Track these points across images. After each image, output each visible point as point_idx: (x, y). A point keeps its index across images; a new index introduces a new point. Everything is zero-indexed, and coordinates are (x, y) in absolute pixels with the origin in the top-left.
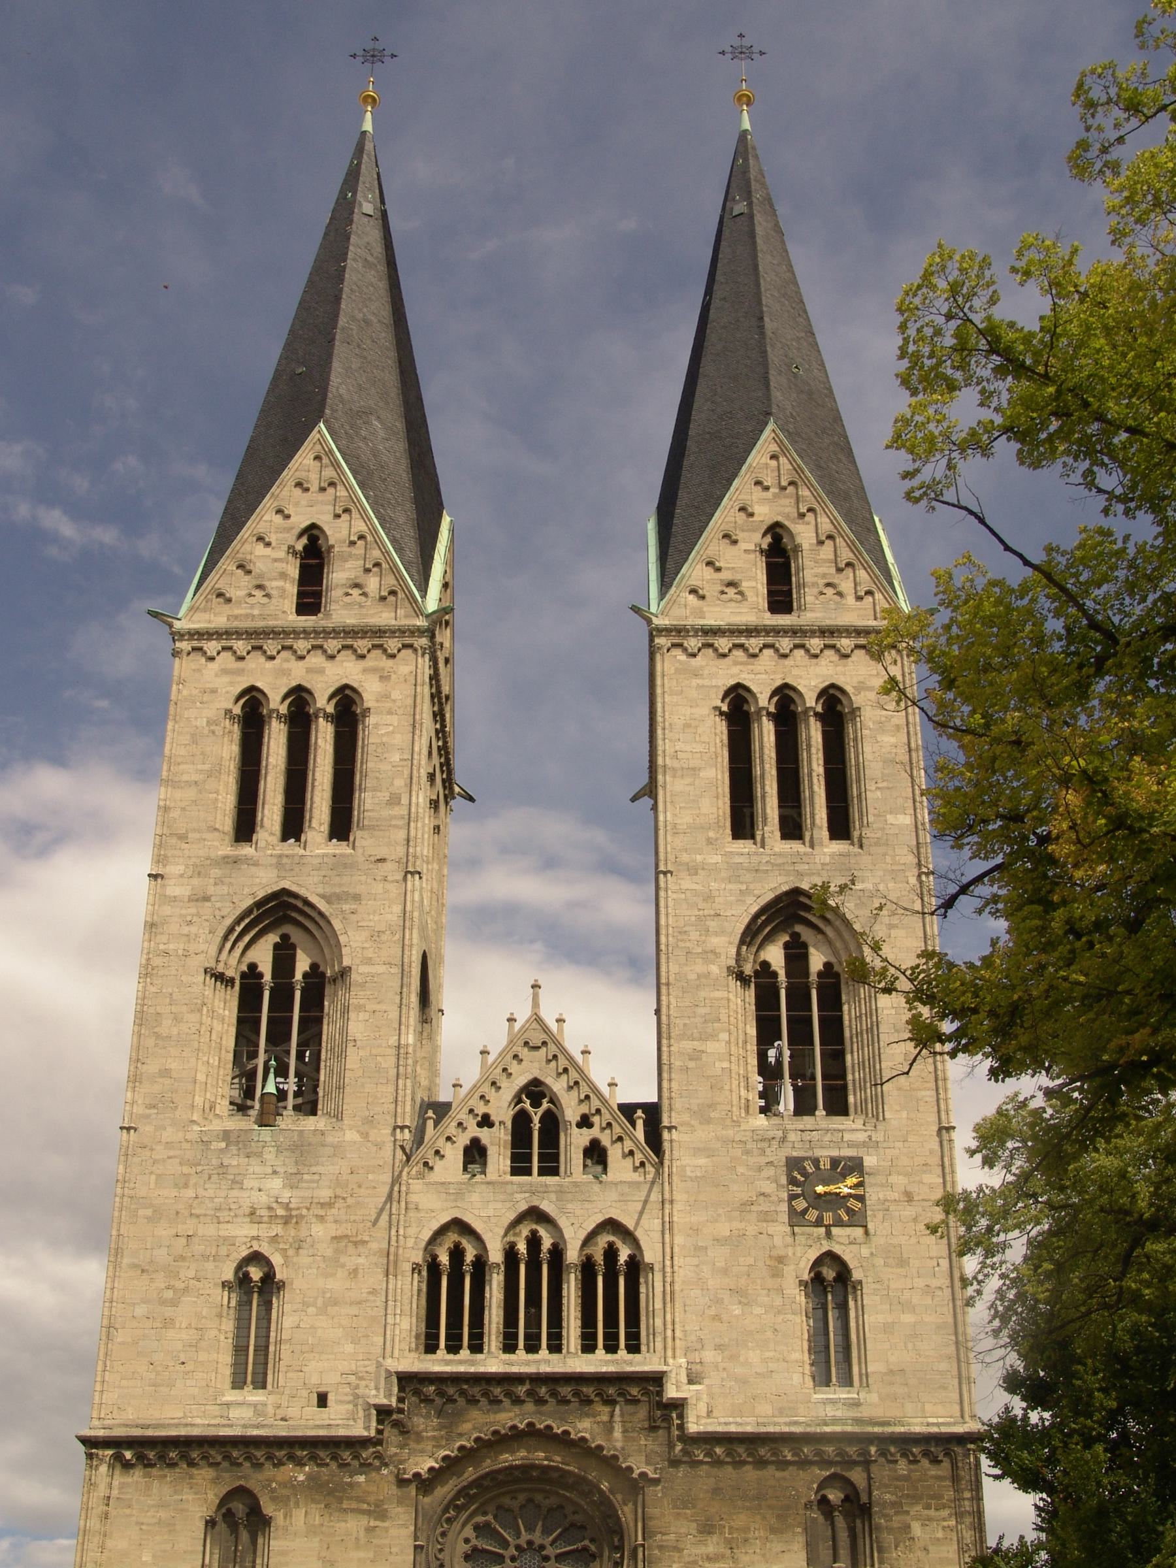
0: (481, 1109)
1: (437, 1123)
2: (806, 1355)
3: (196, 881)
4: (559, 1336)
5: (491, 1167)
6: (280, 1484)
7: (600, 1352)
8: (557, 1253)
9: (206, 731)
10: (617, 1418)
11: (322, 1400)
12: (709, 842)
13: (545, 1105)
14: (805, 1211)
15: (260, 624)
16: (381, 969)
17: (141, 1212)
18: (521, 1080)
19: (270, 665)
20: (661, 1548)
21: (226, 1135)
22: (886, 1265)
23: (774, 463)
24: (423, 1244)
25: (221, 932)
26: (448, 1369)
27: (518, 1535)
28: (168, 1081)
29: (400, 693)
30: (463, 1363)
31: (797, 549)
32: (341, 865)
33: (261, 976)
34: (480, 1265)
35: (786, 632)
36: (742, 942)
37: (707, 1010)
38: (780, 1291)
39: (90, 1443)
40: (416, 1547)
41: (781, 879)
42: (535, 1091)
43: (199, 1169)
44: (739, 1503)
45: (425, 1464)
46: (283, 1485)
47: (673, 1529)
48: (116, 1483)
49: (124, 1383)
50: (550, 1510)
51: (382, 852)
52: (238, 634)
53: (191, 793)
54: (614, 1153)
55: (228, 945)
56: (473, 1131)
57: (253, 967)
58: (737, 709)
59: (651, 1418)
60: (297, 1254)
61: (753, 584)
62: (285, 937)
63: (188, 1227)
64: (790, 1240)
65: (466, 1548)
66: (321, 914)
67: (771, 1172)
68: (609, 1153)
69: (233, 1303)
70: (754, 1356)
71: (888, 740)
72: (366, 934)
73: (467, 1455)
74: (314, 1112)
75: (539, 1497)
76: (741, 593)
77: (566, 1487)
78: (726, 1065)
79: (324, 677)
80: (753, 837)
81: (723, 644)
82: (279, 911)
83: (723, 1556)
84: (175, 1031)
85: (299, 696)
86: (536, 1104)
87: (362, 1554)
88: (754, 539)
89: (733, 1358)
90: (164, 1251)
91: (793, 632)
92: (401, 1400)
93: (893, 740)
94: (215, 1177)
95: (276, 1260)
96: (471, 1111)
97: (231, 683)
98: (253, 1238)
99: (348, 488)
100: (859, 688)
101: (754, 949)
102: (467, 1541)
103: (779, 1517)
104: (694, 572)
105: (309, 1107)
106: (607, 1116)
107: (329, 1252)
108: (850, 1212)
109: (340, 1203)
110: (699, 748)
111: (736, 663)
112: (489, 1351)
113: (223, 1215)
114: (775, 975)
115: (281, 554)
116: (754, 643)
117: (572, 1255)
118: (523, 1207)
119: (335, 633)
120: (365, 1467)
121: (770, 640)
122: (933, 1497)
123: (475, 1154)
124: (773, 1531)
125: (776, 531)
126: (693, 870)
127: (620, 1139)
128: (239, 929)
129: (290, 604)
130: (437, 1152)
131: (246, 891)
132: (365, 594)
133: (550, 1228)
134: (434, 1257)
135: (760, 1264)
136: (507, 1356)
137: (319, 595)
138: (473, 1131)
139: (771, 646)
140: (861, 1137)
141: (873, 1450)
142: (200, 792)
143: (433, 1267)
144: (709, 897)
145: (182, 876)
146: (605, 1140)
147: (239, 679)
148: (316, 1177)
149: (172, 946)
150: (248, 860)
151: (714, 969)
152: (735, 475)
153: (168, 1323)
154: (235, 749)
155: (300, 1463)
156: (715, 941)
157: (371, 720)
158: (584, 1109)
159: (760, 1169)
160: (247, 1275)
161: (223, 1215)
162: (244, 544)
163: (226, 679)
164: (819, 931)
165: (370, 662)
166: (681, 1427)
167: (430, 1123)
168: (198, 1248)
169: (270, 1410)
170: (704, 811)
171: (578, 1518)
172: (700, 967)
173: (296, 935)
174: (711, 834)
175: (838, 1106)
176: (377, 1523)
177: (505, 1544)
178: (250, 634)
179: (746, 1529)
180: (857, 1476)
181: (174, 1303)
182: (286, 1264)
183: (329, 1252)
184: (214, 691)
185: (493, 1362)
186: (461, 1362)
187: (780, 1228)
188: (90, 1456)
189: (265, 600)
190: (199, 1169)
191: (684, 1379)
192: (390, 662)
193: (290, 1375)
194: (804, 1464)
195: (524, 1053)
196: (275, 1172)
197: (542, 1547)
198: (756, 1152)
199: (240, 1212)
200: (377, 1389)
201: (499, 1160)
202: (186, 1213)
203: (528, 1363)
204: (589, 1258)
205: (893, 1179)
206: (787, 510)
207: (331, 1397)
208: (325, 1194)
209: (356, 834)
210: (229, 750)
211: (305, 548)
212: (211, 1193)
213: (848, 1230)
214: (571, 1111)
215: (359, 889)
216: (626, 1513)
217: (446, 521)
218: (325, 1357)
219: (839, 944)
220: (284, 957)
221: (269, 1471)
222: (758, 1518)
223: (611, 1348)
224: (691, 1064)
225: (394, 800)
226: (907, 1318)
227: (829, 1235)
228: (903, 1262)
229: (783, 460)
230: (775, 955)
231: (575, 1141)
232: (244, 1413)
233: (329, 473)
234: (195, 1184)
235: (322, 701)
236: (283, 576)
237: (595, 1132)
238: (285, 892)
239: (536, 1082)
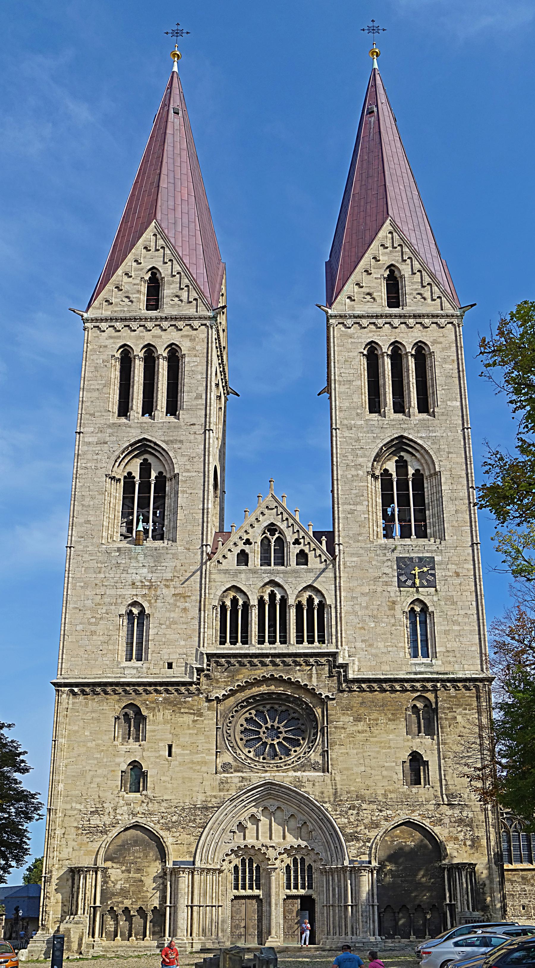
0: (245, 537)
2: (406, 644)
3: (99, 435)
4: (285, 637)
6: (150, 702)
7: (306, 644)
8: (284, 600)
9: (102, 365)
10: (314, 672)
11: (170, 666)
12: (358, 414)
13: (277, 535)
14: (406, 581)
15: (128, 315)
16: (194, 474)
17: (78, 584)
18: (266, 524)
19: (133, 334)
20: (335, 727)
21: (119, 550)
22: (446, 604)
23: (390, 235)
24: (218, 597)
25: (114, 458)
26: (231, 652)
27: (266, 722)
28: (89, 526)
29: (201, 347)
30: (239, 648)
31: (402, 277)
34: (246, 606)
35: (396, 316)
36: (374, 460)
37: (357, 491)
38: (394, 616)
40: (217, 728)
42: (272, 528)
43: (106, 565)
44: (374, 708)
45: (220, 693)
46: (152, 702)
47: (341, 720)
48: (70, 702)
49: (73, 659)
50: (282, 711)
51: (193, 421)
53: (96, 394)
54: (311, 555)
55: (117, 464)
56: (241, 546)
58: (372, 354)
59: (330, 672)
60: (156, 602)
61: (380, 294)
64: (398, 594)
65: (242, 729)
67: (389, 563)
68: (309, 556)
69: (125, 624)
70: (381, 645)
71: (448, 366)
72: (187, 458)
73: (241, 689)
74: (162, 539)
75: (276, 706)
76: (374, 299)
77: (289, 702)
78: (366, 516)
80: (379, 412)
81: (365, 322)
83: (366, 731)
84: (92, 503)
85: (150, 349)
86: (273, 534)
87: (191, 731)
89: (371, 645)
90: (90, 601)
92: (208, 665)
93: (451, 367)
94: (114, 569)
95: (146, 605)
96: (240, 538)
97: (114, 343)
98: (134, 595)
100: (434, 342)
101: (380, 464)
102: (242, 725)
103: (392, 714)
105: (159, 536)
106: (307, 540)
107: (171, 601)
108: (427, 581)
109: (176, 579)
111: (371, 332)
112: (251, 643)
113: (119, 585)
114: (391, 475)
115: (138, 281)
116: (380, 322)
117: (292, 601)
118: (267, 580)
120: (191, 693)
121: (388, 320)
122: (467, 705)
124: (390, 720)
125: (391, 268)
128: (122, 457)
129: (143, 305)
130: (224, 556)
131: (125, 439)
132: (181, 301)
133: (280, 589)
134: (224, 603)
135: (384, 604)
136: (259, 646)
137: (157, 301)
138: (241, 546)
139: (389, 323)
140: (434, 548)
141: (439, 685)
143: (223, 607)
144: (358, 440)
145: (92, 432)
146: (307, 551)
147: (118, 341)
148: (164, 568)
149: (89, 465)
150: (126, 425)
151: (361, 473)
153: (93, 633)
159: (384, 562)
160: (131, 611)
161: (119, 585)
163: (111, 341)
166: (345, 676)
168: (107, 600)
169: (145, 670)
170: (355, 400)
171: (295, 715)
172: (354, 472)
174: (359, 411)
175: (422, 534)
176: (198, 718)
177: (261, 727)
178: (122, 320)
179: (377, 720)
180: (430, 696)
181: (96, 624)
182: (150, 606)
183: (171, 601)
184: (106, 346)
185: (254, 648)
186: (237, 649)
187: (394, 588)
188: (58, 691)
189: (130, 303)
190: (106, 565)
191: (347, 655)
192: (195, 332)
193: (154, 655)
194: (405, 690)
195: (266, 511)
196: (144, 566)
197: (278, 728)
198: (381, 555)
199: (127, 584)
200: (196, 661)
201: (255, 559)
202: (100, 584)
203: (271, 648)
204: (300, 602)
205: (449, 566)
206: (397, 258)
207: (174, 664)
208: (169, 576)
210: (115, 374)
211: (150, 278)
212: (112, 575)
213: (427, 589)
214: (290, 538)
215: (182, 438)
216: (318, 711)
218: (170, 647)
219: (423, 461)
220: (145, 468)
222: (383, 715)
223: (311, 642)
224: (349, 516)
225: (198, 397)
226: (456, 628)
227: (417, 591)
228: (454, 603)
229: (395, 234)
232: (132, 671)
233: (161, 242)
234: (104, 572)
235: (162, 351)
236: (139, 292)
237: (301, 546)
239: (272, 524)
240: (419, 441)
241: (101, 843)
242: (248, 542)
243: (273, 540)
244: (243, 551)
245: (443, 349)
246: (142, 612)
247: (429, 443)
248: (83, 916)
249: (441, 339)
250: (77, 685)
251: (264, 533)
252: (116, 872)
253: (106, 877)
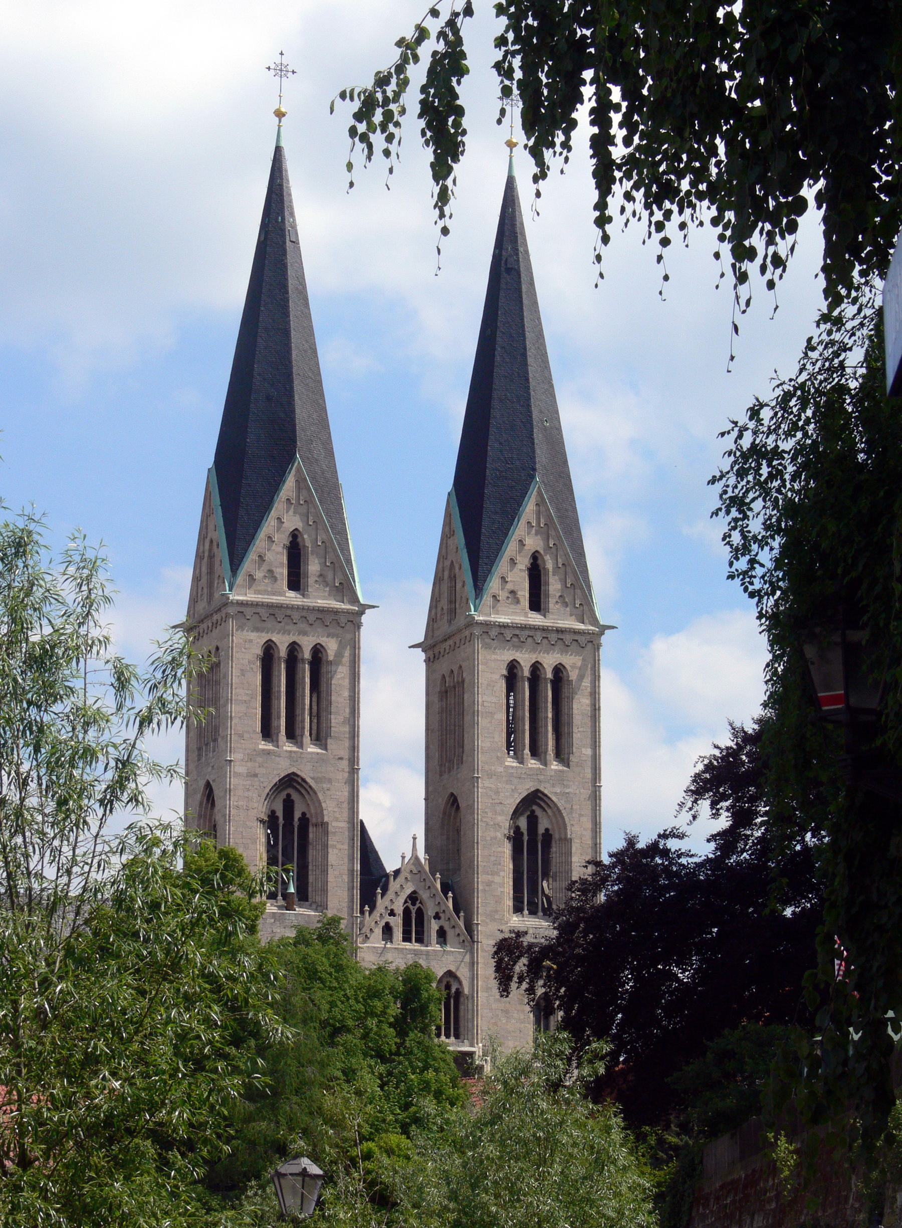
1: (371, 913)
3: (249, 764)
5: (395, 939)
13: (418, 905)
32: (320, 759)
33: (277, 818)
41: (531, 784)
42: (413, 898)
54: (450, 934)
57: (273, 812)
62: (289, 795)
66: (310, 787)
82: (290, 783)
85: (294, 648)
86: (414, 904)
88: (524, 563)
91: (544, 629)
97: (260, 637)
110: (494, 700)
123: (388, 931)
125: (535, 557)
126: (490, 775)
127: (454, 927)
131: (275, 772)
142: (248, 707)
146: (446, 928)
147: (263, 634)
158: (437, 909)
164: (544, 810)
167: (367, 914)
172: (492, 834)
173: (295, 796)
201: (398, 933)
210: (257, 679)
214: (430, 912)
219: (554, 820)
224: (487, 888)
230: (523, 823)
231: (434, 926)
237: (442, 922)
238: (294, 774)
239: (414, 892)
240: (554, 798)
242: (392, 913)
243: (413, 909)
244: (387, 924)
247: (563, 802)
251: (406, 902)
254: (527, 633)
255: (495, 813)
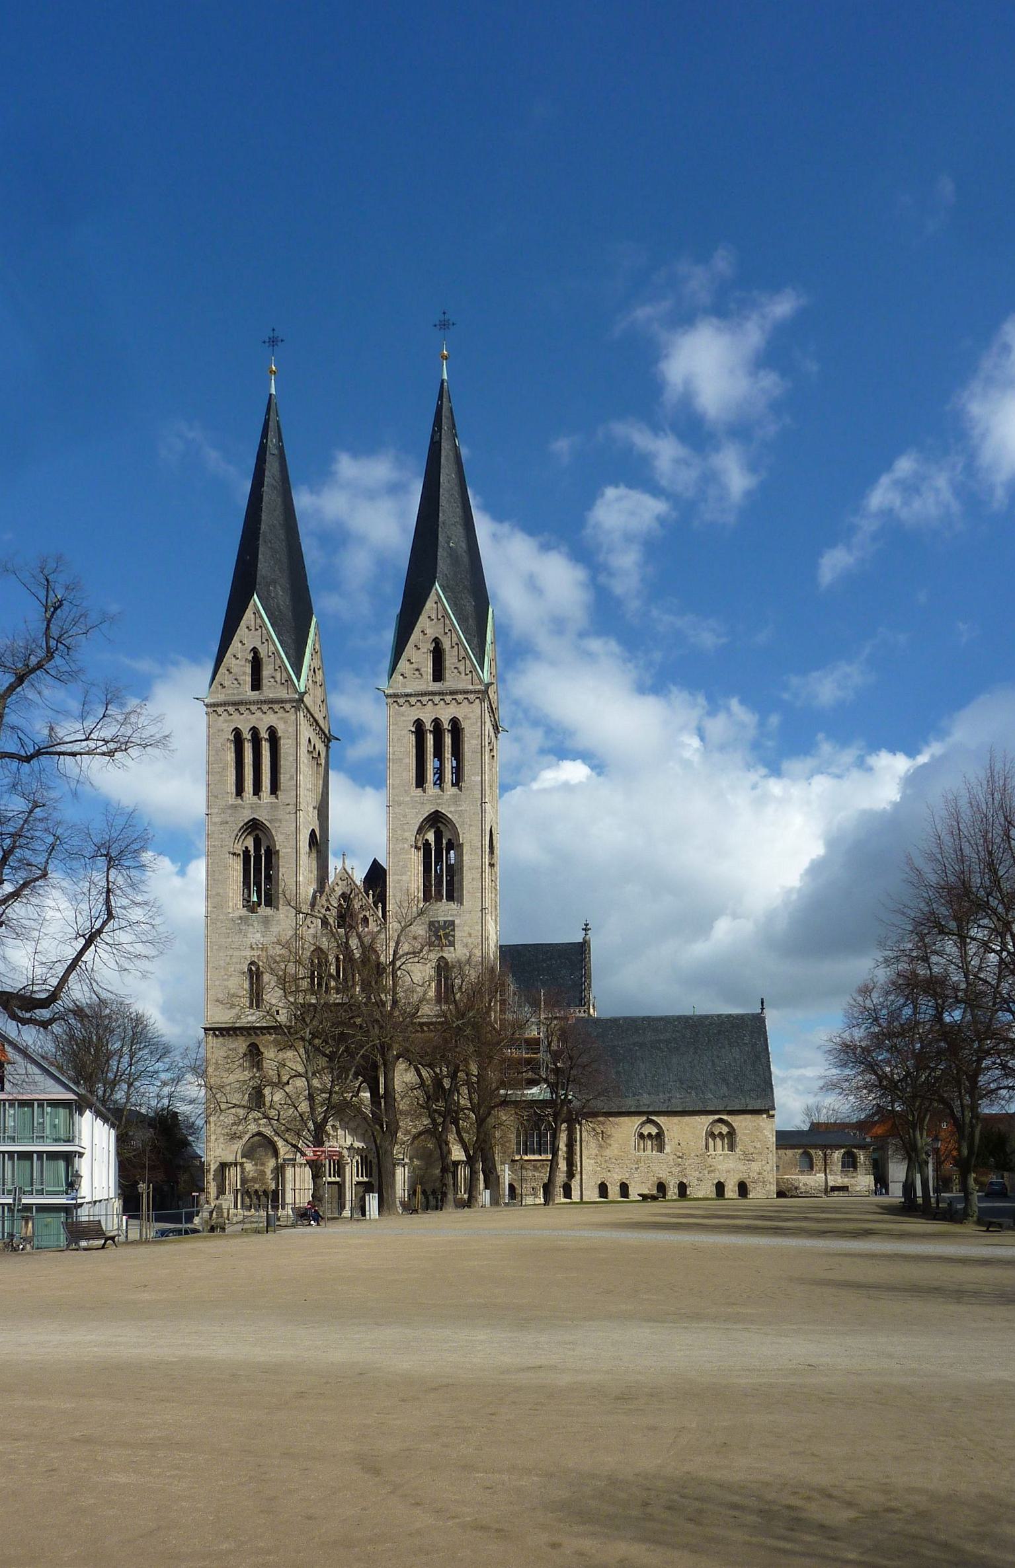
21: (240, 918)
32: (274, 807)
39: (206, 1029)
52: (229, 704)
54: (371, 919)
62: (257, 835)
63: (230, 952)
71: (474, 742)
79: (264, 721)
81: (413, 700)
85: (255, 731)
91: (440, 693)
99: (267, 629)
100: (465, 718)
104: (403, 665)
115: (243, 663)
116: (425, 699)
119: (265, 702)
125: (436, 641)
152: (420, 613)
154: (233, 755)
155: (270, 1034)
156: (407, 834)
157: (282, 742)
162: (228, 659)
165: (279, 715)
181: (227, 980)
195: (340, 882)
209: (279, 793)
210: (231, 756)
215: (280, 817)
217: (314, 620)
221: (262, 1037)
225: (291, 778)
230: (431, 836)
235: (264, 735)
241: (238, 1145)
242: (328, 909)
245: (472, 724)
246: (258, 969)
248: (229, 1196)
249: (471, 715)
250: (217, 1029)
252: (249, 1166)
253: (243, 1170)
254: (428, 698)
255: (404, 831)
